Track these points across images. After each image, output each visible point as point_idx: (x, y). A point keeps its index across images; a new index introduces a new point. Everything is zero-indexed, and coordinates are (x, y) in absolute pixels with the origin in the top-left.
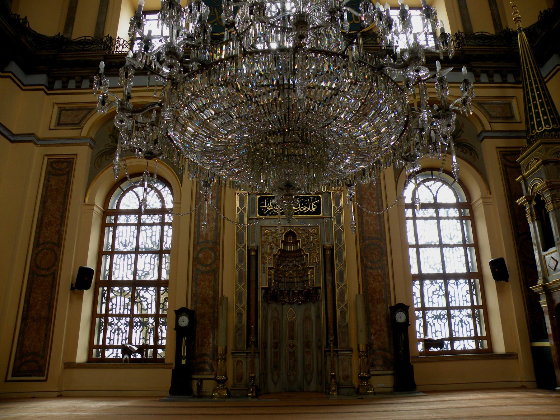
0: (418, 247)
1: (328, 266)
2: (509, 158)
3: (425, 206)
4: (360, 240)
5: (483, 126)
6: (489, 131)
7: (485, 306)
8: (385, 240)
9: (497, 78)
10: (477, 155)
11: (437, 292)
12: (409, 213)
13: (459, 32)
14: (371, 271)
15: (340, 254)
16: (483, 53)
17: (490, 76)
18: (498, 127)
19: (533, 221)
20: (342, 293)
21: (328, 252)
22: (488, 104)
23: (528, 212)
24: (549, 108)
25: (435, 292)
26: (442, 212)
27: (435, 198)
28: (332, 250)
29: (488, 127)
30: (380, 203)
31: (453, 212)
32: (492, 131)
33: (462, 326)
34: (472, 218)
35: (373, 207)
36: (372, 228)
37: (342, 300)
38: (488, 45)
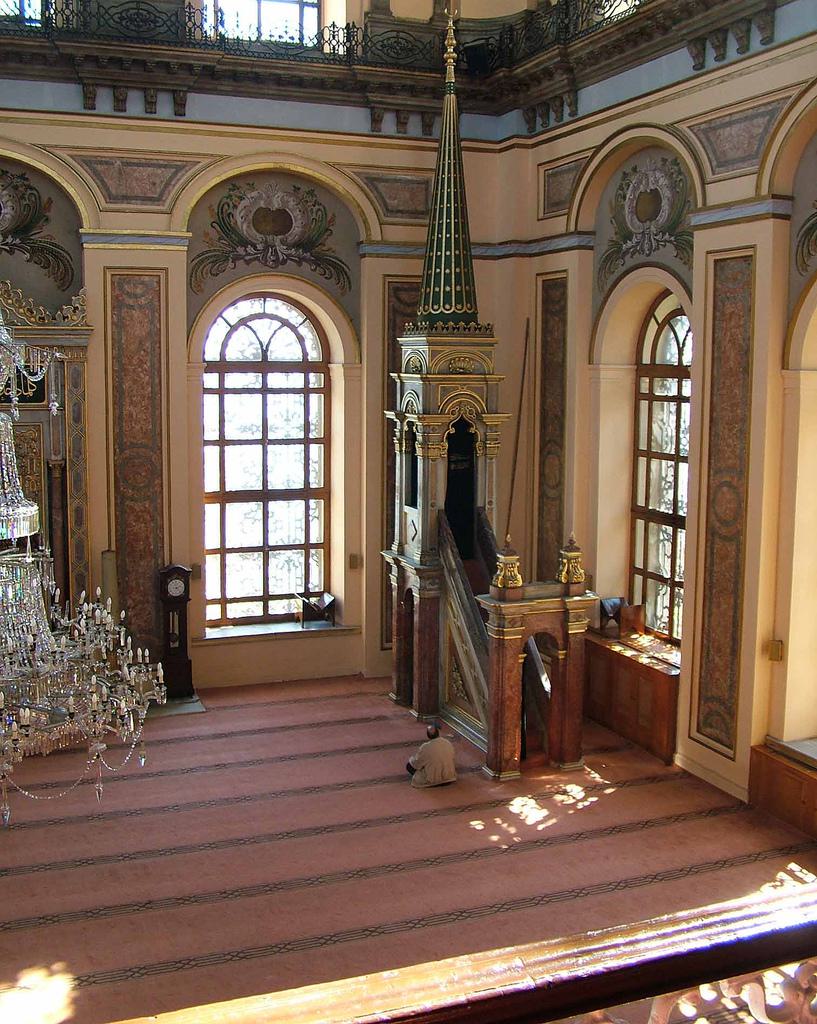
0: (222, 442)
1: (57, 496)
2: (404, 296)
3: (243, 367)
4: (115, 450)
5: (368, 229)
6: (378, 243)
7: (326, 545)
8: (160, 449)
9: (414, 126)
10: (350, 283)
11: (253, 514)
12: (211, 380)
13: (354, 26)
14: (132, 504)
15: (79, 480)
16: (392, 81)
17: (402, 124)
18: (398, 233)
19: (401, 451)
20: (80, 547)
21: (57, 474)
22: (387, 181)
23: (398, 434)
24: (458, 270)
25: (249, 514)
26: (276, 380)
27: (265, 352)
28: (64, 469)
29: (376, 235)
30: (157, 381)
31: (296, 380)
32: (384, 243)
33: (289, 570)
34: (326, 391)
35: (143, 388)
36: (138, 427)
37: (80, 558)
38: (405, 67)
